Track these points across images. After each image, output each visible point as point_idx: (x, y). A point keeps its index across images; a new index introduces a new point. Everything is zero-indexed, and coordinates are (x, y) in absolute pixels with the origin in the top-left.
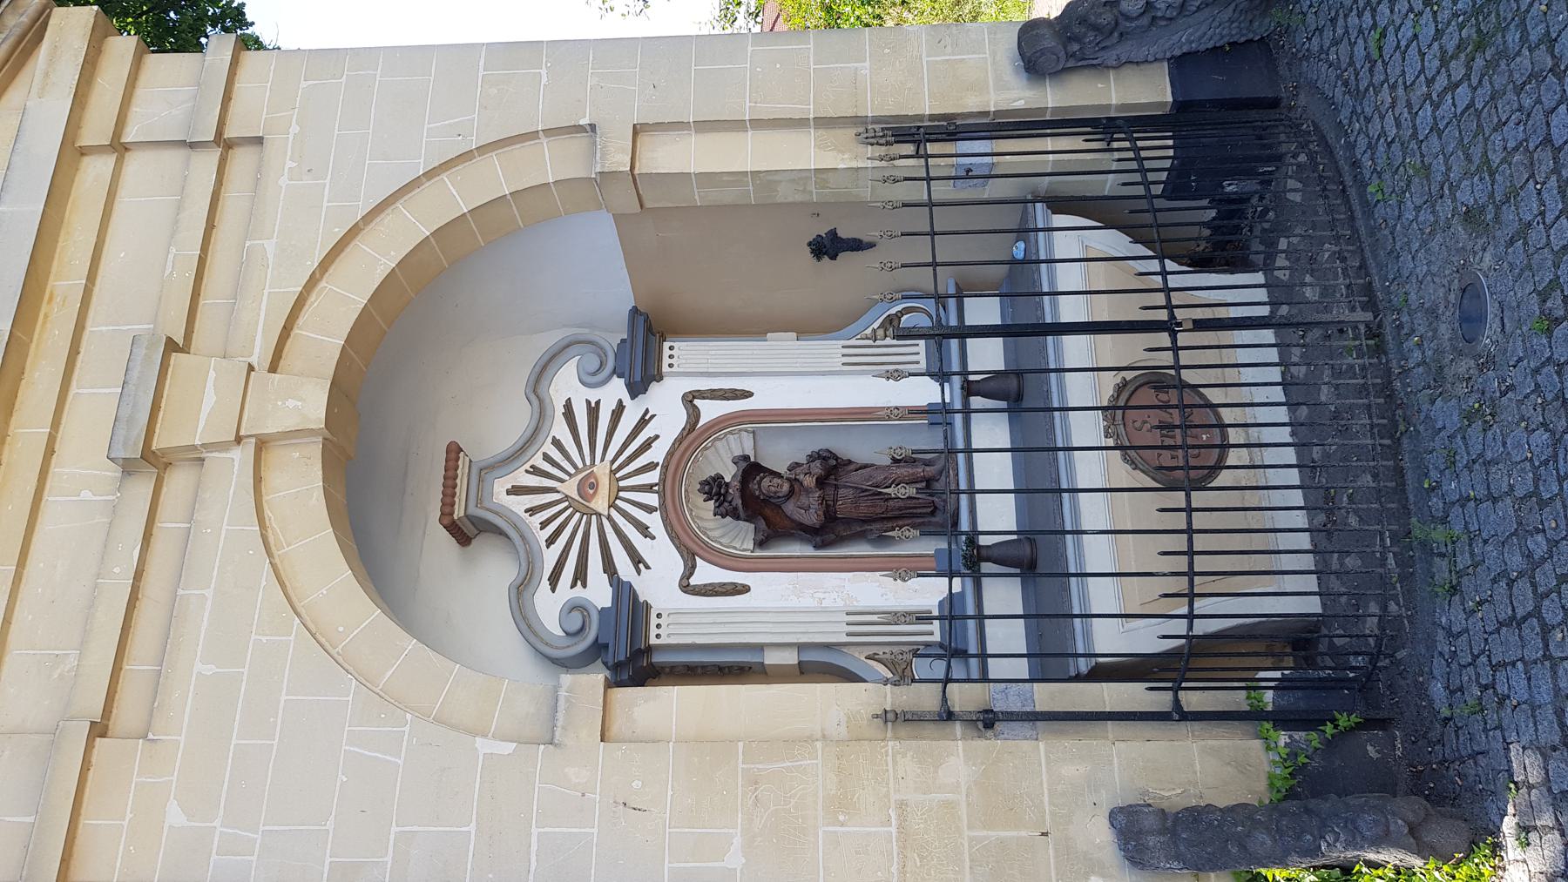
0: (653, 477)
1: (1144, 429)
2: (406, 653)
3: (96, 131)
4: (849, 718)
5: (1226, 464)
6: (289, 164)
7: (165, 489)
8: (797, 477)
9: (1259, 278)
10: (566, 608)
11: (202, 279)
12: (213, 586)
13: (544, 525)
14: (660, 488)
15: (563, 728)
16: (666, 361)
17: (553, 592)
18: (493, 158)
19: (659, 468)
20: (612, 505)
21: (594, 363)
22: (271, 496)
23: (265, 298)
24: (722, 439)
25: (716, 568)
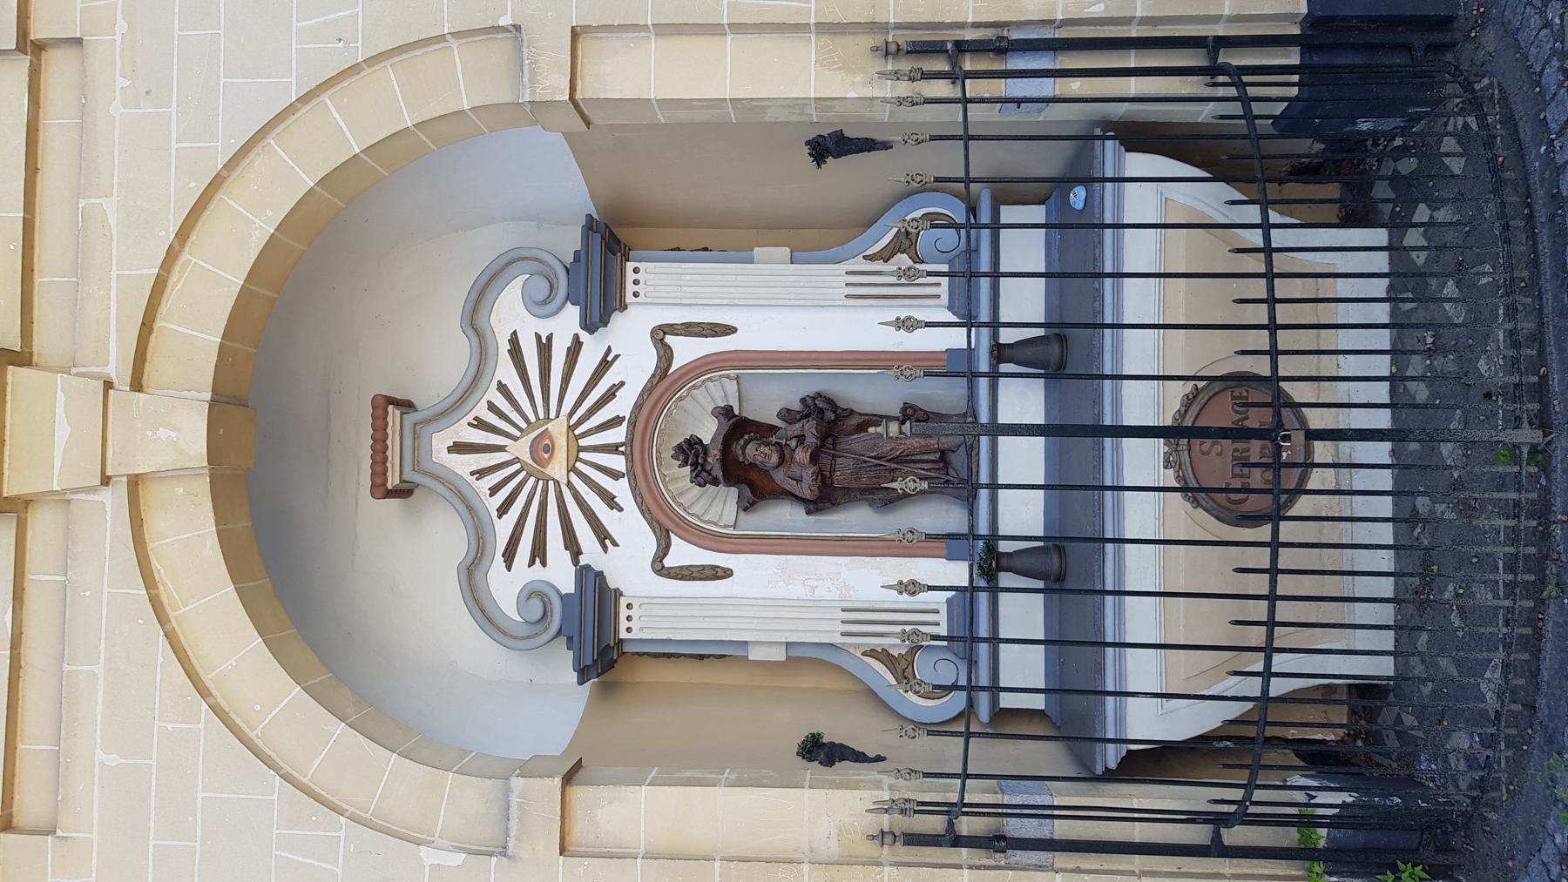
0: (618, 435)
1: (1213, 453)
2: (334, 739)
4: (840, 830)
5: (1308, 488)
6: (121, 82)
7: (30, 533)
8: (788, 443)
9: (1380, 236)
10: (525, 594)
11: (33, 247)
12: (102, 661)
13: (494, 490)
14: (623, 448)
15: (517, 839)
16: (630, 288)
17: (509, 570)
18: (388, 72)
19: (625, 424)
20: (572, 469)
21: (542, 289)
22: (157, 543)
23: (114, 284)
24: (701, 386)
25: (695, 547)
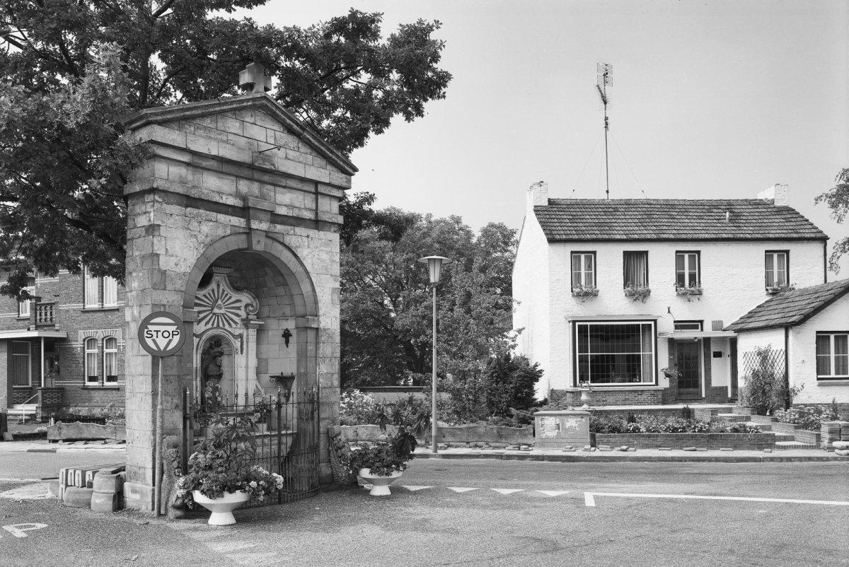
3: (321, 189)
20: (214, 314)
